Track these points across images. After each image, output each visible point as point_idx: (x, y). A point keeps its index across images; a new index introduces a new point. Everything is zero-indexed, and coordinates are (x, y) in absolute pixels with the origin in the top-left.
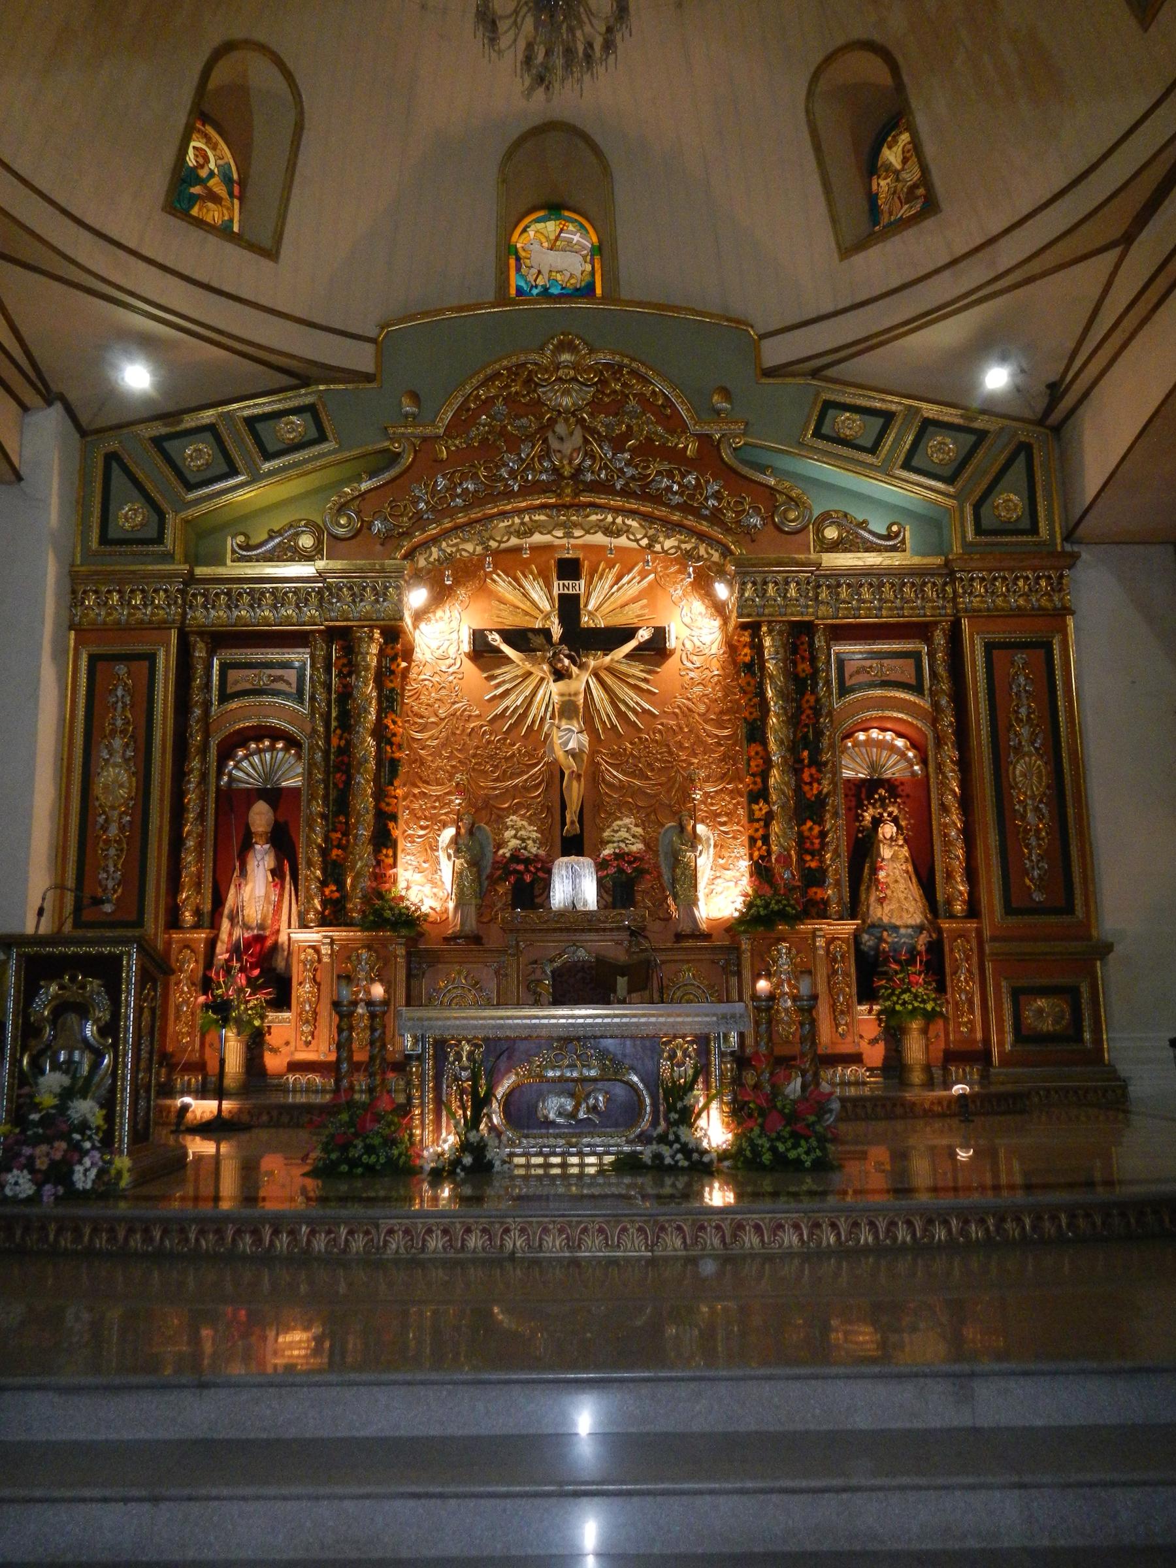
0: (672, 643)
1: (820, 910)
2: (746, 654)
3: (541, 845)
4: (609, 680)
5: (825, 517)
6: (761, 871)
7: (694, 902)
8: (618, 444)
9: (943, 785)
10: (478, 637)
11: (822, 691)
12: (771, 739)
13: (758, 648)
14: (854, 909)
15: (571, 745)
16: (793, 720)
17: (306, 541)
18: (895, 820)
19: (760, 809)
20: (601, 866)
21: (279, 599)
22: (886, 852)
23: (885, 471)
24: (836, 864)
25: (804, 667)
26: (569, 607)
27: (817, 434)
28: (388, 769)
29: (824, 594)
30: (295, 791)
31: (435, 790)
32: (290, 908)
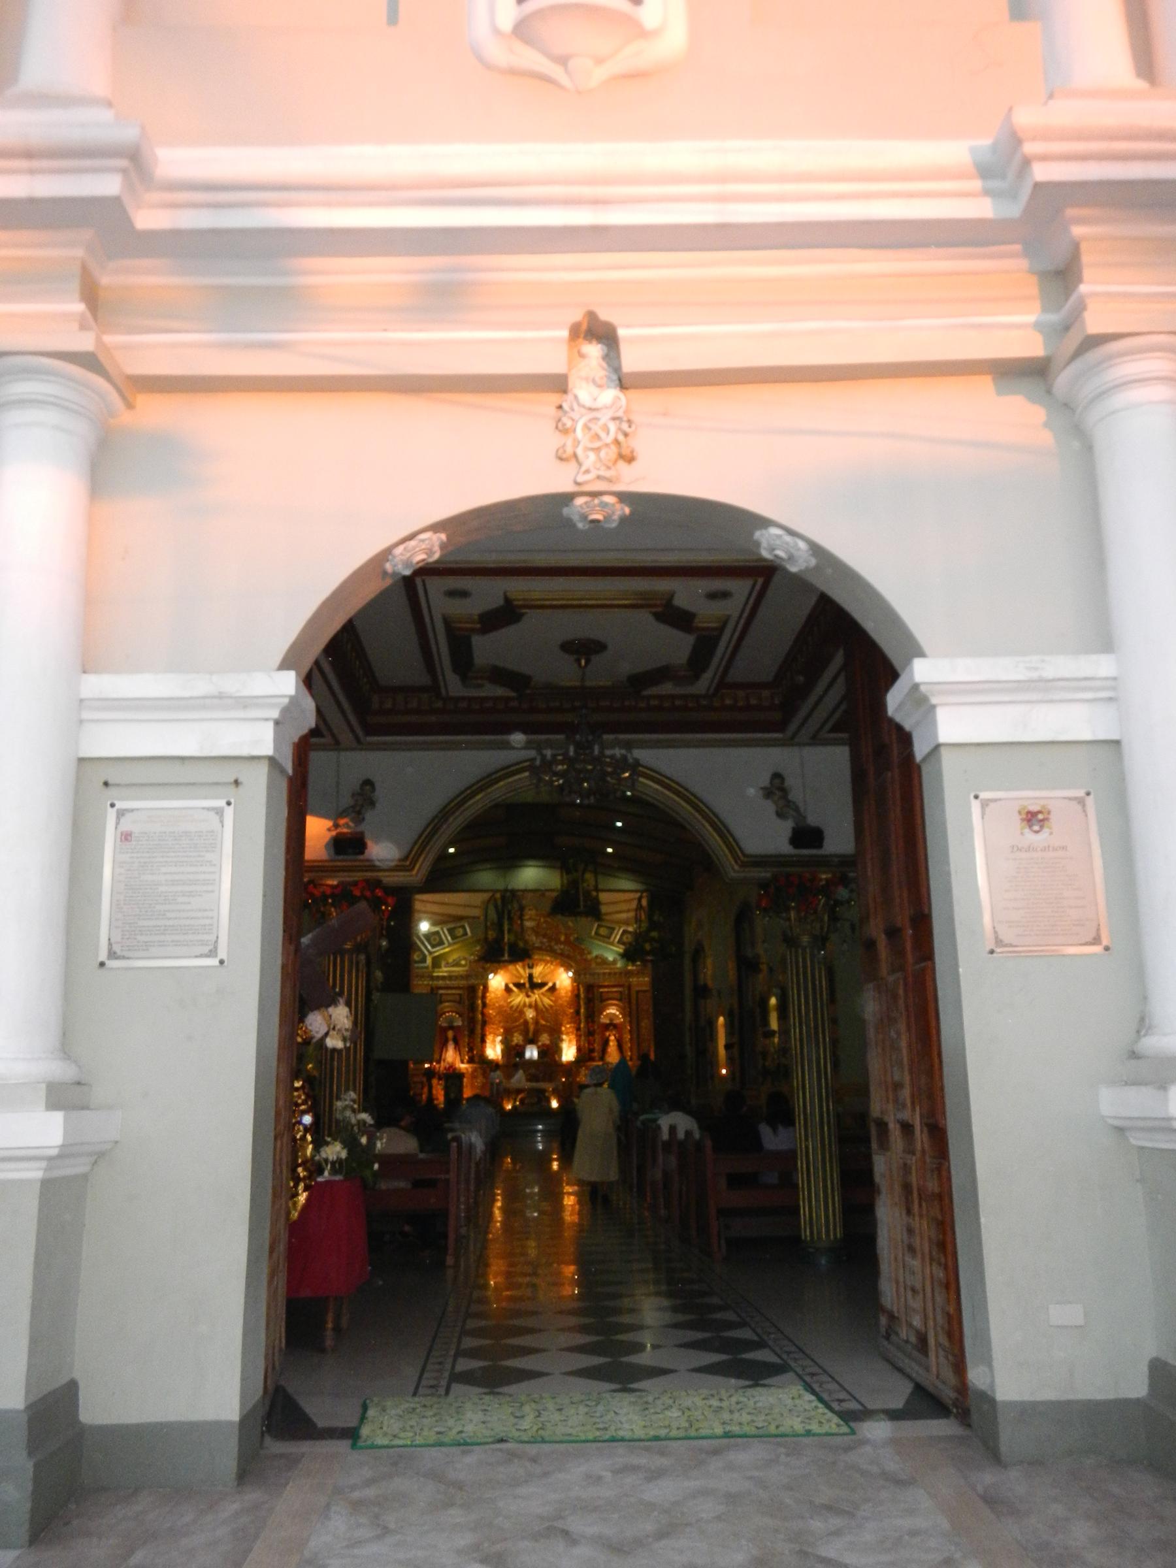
0: (558, 986)
1: (593, 1059)
2: (576, 992)
3: (523, 1041)
4: (542, 996)
5: (597, 957)
6: (579, 1050)
7: (560, 1056)
8: (544, 936)
9: (626, 1027)
10: (507, 986)
11: (596, 1002)
12: (582, 1015)
13: (579, 990)
14: (602, 1058)
15: (531, 1016)
16: (587, 1009)
17: (463, 962)
18: (615, 1035)
19: (579, 1033)
20: (538, 1048)
21: (456, 978)
22: (611, 1044)
23: (612, 944)
24: (597, 1046)
25: (590, 996)
26: (531, 977)
27: (596, 933)
28: (484, 1023)
29: (596, 976)
30: (458, 1027)
31: (495, 1027)
32: (458, 1059)
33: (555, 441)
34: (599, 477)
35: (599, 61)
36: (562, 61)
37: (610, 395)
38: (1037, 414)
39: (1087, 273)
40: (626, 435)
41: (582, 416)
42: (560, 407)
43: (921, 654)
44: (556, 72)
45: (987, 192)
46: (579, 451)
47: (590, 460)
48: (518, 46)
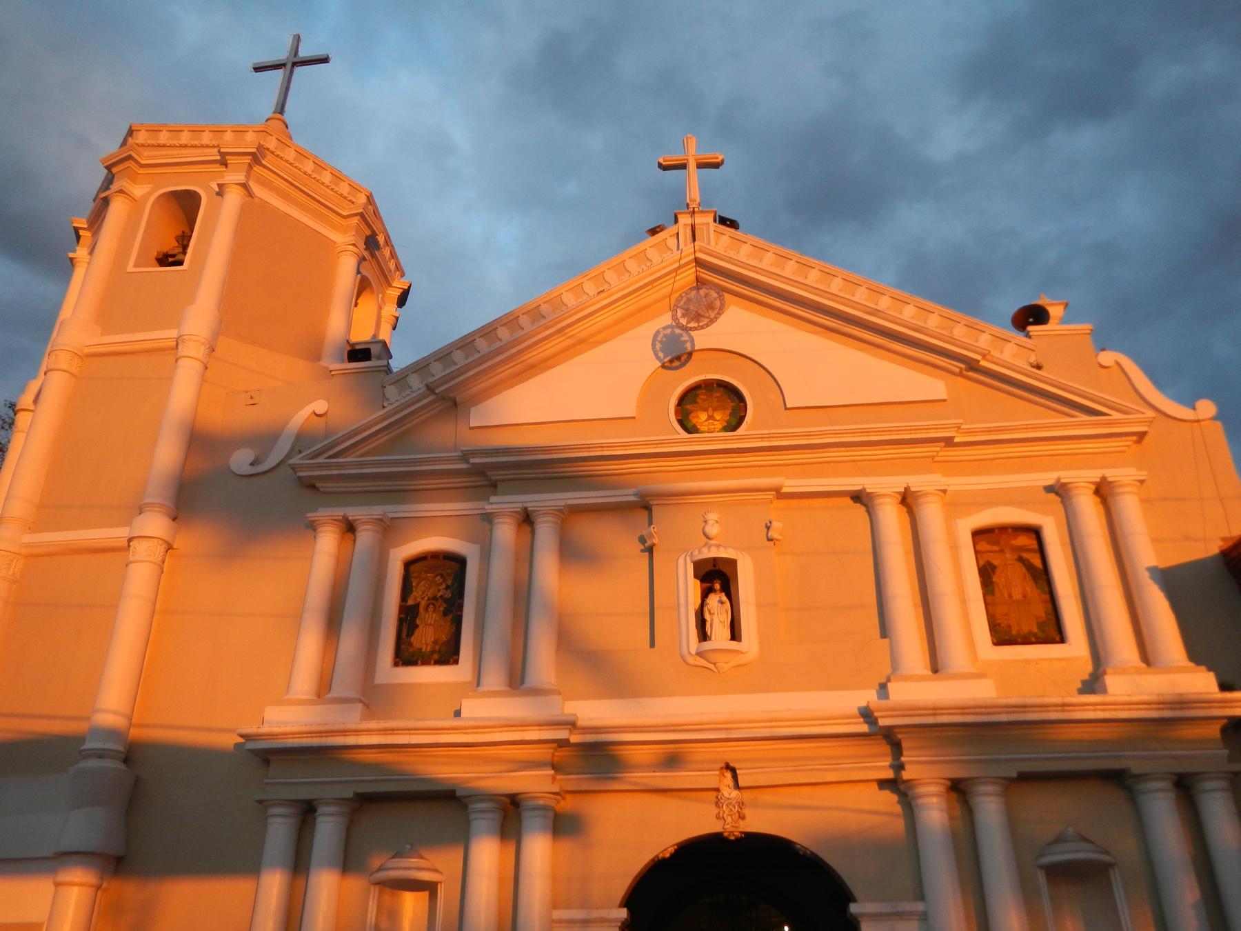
33: (715, 811)
34: (733, 826)
35: (727, 663)
36: (715, 664)
37: (735, 793)
38: (894, 798)
39: (905, 753)
40: (741, 808)
41: (725, 801)
42: (717, 797)
43: (855, 900)
44: (712, 666)
45: (865, 722)
46: (725, 816)
47: (729, 819)
48: (698, 658)
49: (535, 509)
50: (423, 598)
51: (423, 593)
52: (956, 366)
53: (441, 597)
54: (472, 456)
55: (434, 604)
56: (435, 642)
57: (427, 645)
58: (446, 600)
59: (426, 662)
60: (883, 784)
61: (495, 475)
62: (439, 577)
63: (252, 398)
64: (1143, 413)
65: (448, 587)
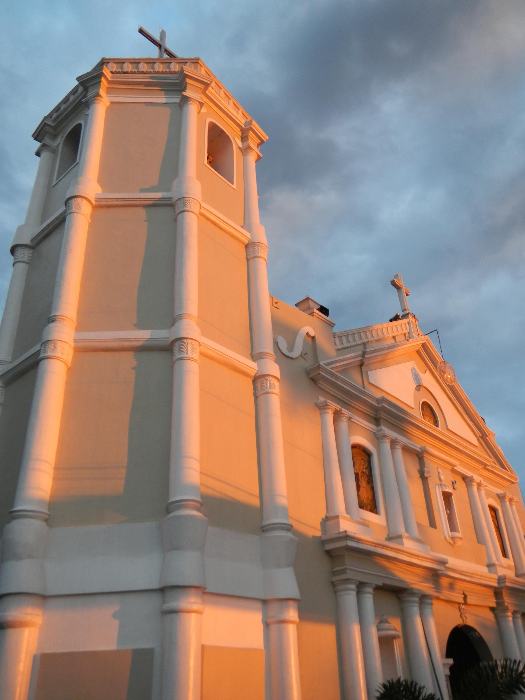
36: (454, 543)
49: (399, 441)
50: (359, 470)
51: (359, 467)
52: (479, 434)
53: (365, 472)
54: (385, 402)
55: (363, 476)
56: (368, 498)
57: (365, 499)
58: (368, 476)
59: (367, 510)
60: (492, 609)
61: (383, 415)
62: (362, 461)
63: (276, 303)
64: (516, 476)
65: (366, 468)
